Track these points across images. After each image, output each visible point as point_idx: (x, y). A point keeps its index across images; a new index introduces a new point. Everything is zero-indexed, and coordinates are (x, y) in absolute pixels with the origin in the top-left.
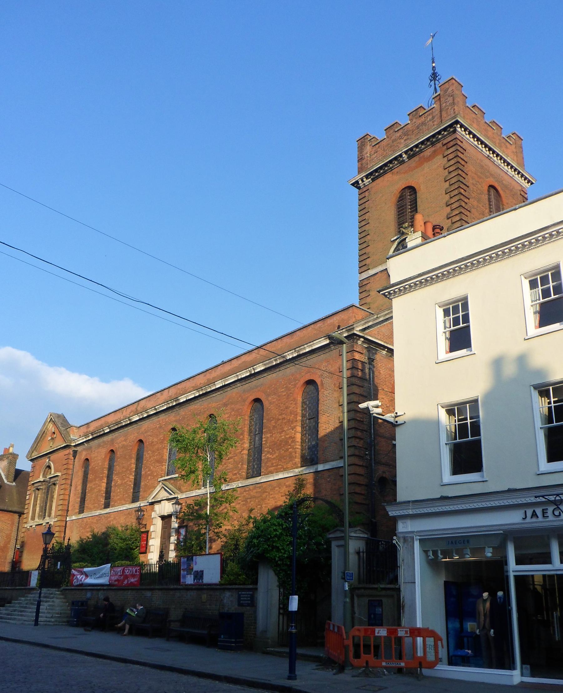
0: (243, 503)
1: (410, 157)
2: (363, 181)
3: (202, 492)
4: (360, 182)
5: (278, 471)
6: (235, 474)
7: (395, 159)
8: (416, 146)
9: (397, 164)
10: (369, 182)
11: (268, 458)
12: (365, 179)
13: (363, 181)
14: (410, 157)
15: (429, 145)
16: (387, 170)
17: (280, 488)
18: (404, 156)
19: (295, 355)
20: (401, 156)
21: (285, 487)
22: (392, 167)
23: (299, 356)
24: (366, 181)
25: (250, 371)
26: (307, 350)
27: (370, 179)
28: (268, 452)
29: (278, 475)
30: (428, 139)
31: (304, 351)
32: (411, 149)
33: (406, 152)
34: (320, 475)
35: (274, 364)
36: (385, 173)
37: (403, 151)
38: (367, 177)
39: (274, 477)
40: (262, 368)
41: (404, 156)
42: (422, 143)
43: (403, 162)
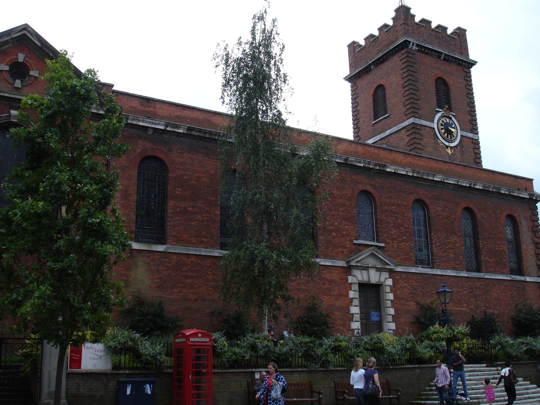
0: (469, 290)
1: (445, 59)
2: (413, 45)
3: (424, 271)
4: (411, 44)
5: (496, 273)
6: (457, 264)
7: (438, 52)
8: (452, 57)
9: (436, 56)
10: (415, 49)
11: (487, 260)
12: (415, 45)
13: (413, 45)
14: (445, 59)
15: (456, 63)
16: (430, 53)
17: (500, 286)
18: (443, 55)
19: (507, 193)
20: (442, 53)
21: (503, 286)
22: (433, 55)
23: (509, 195)
24: (415, 48)
25: (470, 184)
26: (515, 194)
27: (417, 48)
28: (486, 256)
29: (499, 276)
30: (459, 59)
31: (513, 194)
32: (449, 56)
33: (445, 55)
34: (527, 284)
35: (491, 190)
36: (427, 54)
37: (445, 52)
38: (417, 45)
39: (496, 276)
40: (481, 188)
41: (443, 55)
42: (455, 58)
43: (439, 58)
